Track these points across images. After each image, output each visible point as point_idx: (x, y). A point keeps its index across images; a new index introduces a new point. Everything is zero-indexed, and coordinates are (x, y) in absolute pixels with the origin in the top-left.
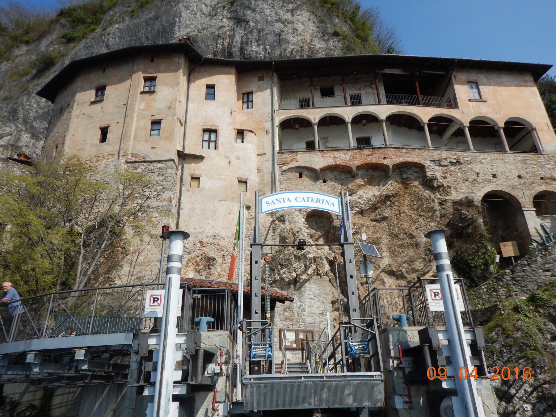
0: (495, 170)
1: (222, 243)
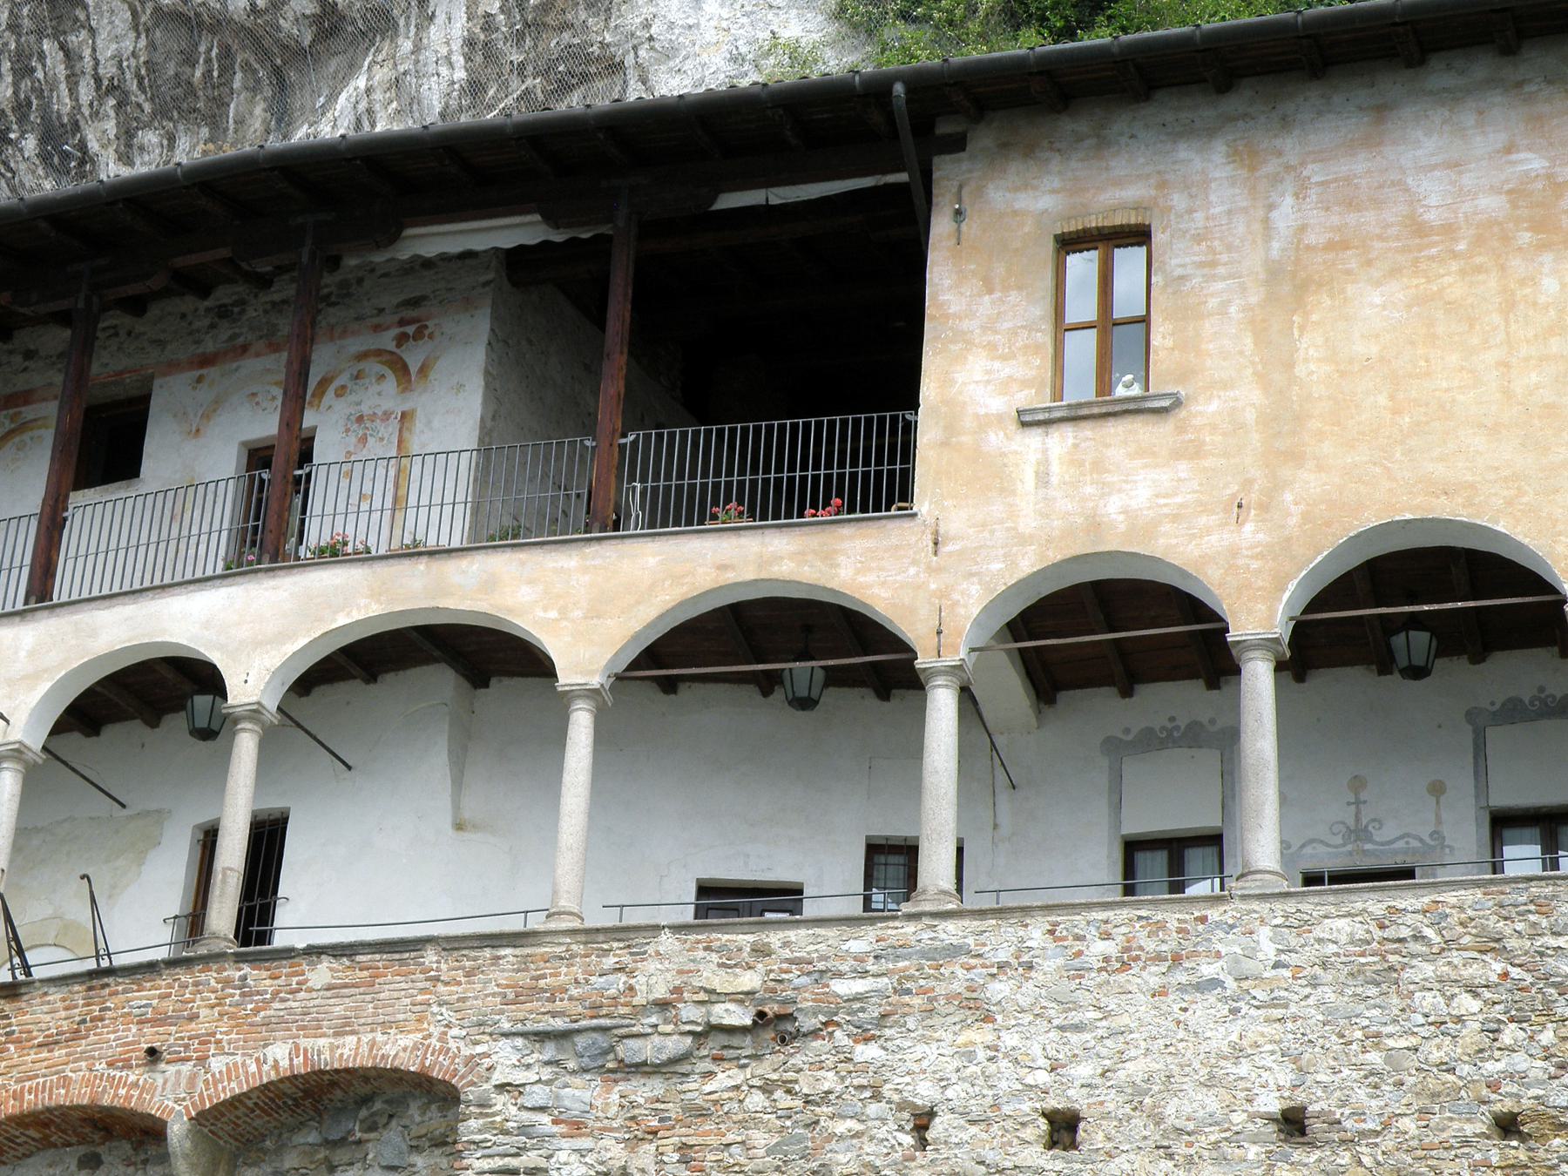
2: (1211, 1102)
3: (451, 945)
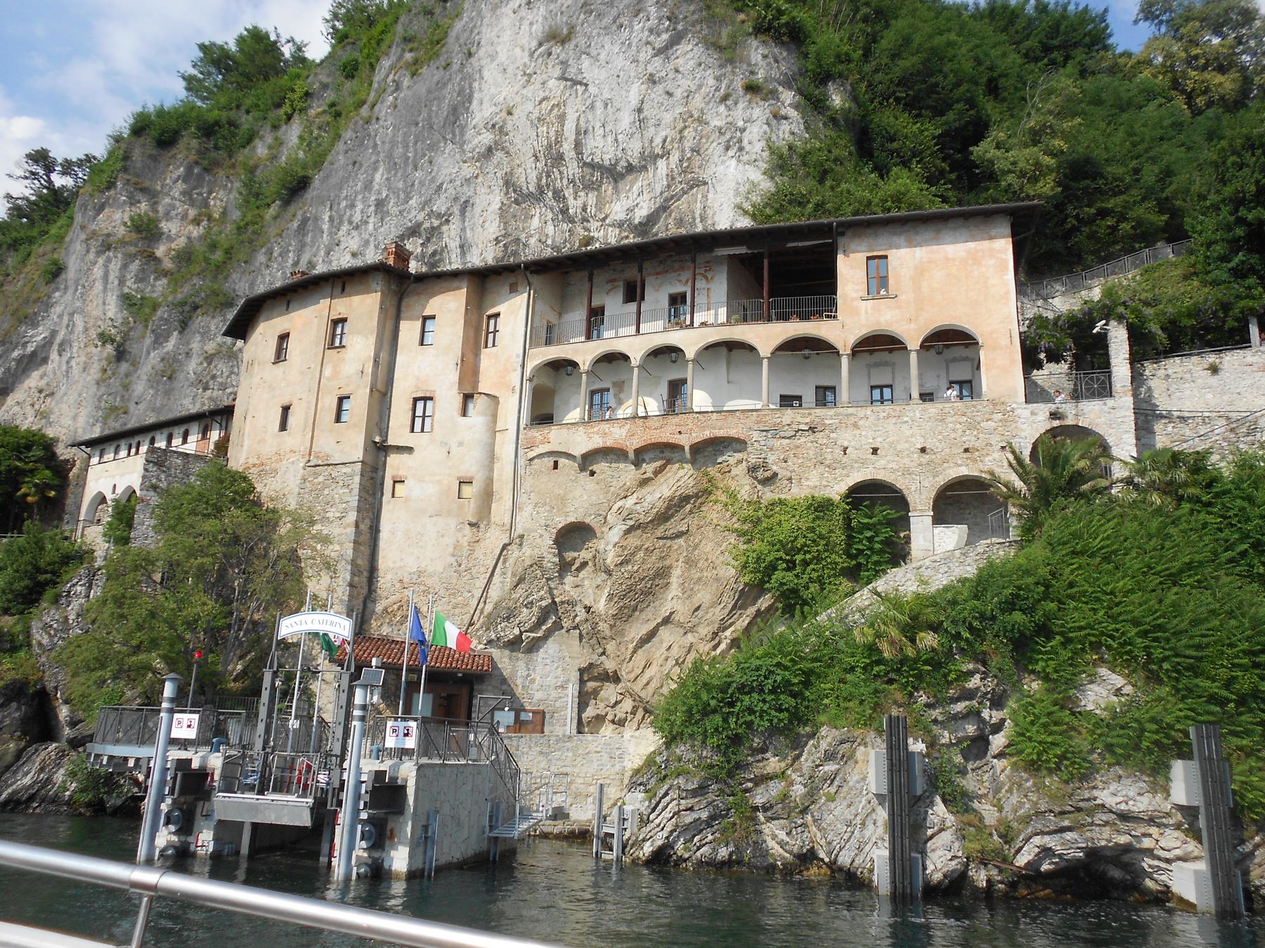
0: (879, 439)
1: (429, 582)
2: (907, 445)
3: (743, 411)
